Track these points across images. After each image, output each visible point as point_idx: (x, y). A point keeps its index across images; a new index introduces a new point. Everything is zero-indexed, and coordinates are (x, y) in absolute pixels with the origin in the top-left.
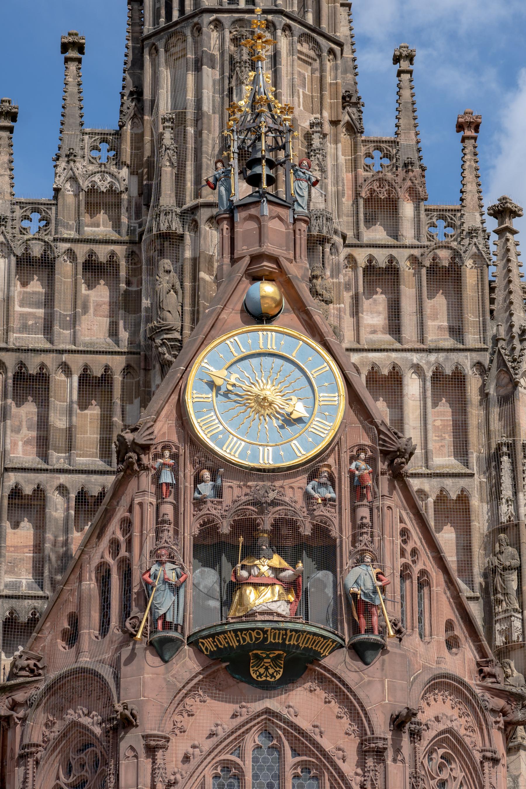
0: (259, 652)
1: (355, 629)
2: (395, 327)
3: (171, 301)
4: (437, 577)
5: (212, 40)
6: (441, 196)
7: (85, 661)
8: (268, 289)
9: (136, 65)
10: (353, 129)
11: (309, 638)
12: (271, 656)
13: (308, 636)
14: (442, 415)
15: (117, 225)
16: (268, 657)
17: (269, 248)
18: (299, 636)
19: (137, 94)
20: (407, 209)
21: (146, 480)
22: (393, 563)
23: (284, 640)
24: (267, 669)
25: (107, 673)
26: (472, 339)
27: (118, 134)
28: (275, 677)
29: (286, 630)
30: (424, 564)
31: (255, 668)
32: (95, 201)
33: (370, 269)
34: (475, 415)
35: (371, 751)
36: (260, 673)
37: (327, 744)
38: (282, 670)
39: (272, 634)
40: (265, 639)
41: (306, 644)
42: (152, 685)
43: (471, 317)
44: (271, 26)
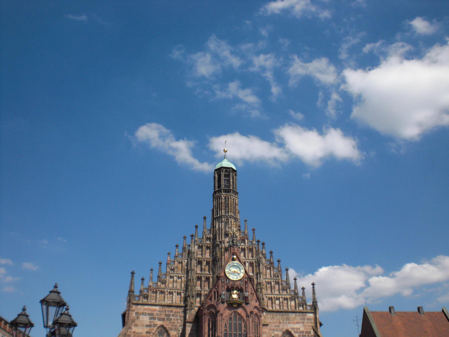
1: (246, 301)
2: (245, 256)
3: (218, 253)
4: (255, 294)
5: (223, 219)
6: (251, 239)
7: (212, 303)
8: (235, 257)
9: (213, 221)
10: (240, 230)
14: (251, 268)
15: (210, 241)
17: (235, 251)
19: (213, 225)
20: (246, 241)
21: (220, 281)
22: (250, 292)
25: (215, 305)
26: (254, 258)
27: (211, 229)
32: (208, 239)
33: (242, 248)
34: (255, 268)
35: (247, 316)
37: (242, 315)
42: (222, 307)
43: (254, 255)
44: (230, 218)
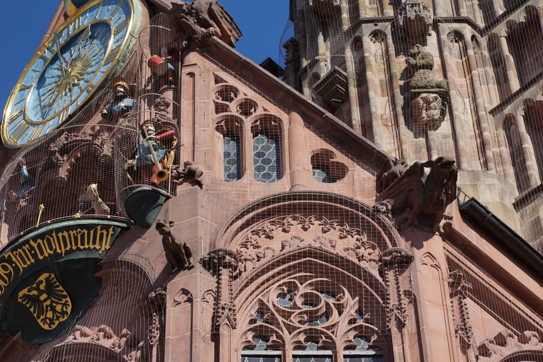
0: (25, 291)
11: (64, 237)
12: (42, 287)
13: (60, 235)
16: (41, 292)
18: (49, 241)
23: (35, 256)
24: (53, 309)
28: (66, 313)
29: (27, 242)
30: (265, 110)
31: (42, 317)
36: (49, 319)
38: (68, 299)
39: (18, 257)
40: (16, 269)
41: (66, 246)
